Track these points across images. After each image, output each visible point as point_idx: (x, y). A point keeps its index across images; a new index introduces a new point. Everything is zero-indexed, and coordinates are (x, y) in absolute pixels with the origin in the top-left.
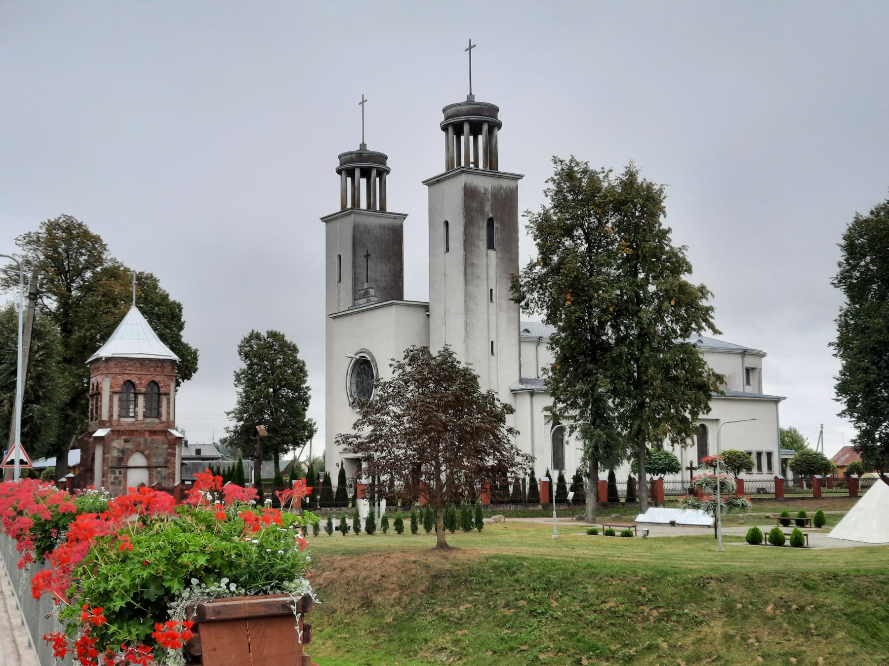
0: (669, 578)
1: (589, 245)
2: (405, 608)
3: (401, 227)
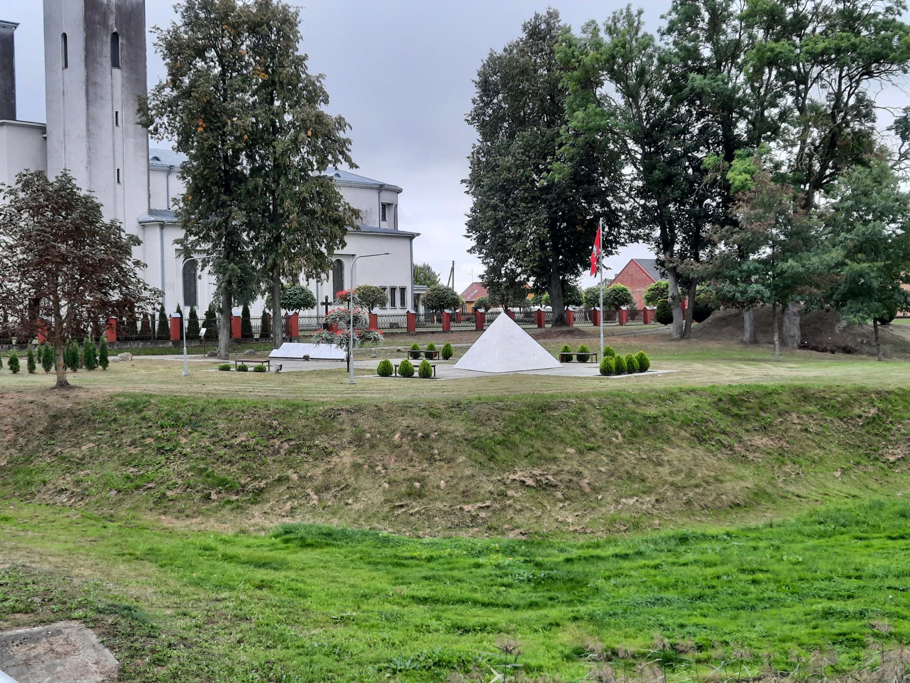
0: (300, 411)
1: (223, 68)
2: (21, 450)
3: (12, 36)
